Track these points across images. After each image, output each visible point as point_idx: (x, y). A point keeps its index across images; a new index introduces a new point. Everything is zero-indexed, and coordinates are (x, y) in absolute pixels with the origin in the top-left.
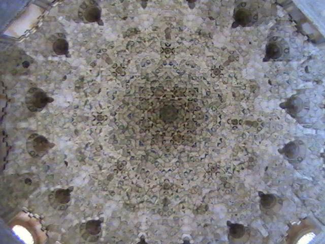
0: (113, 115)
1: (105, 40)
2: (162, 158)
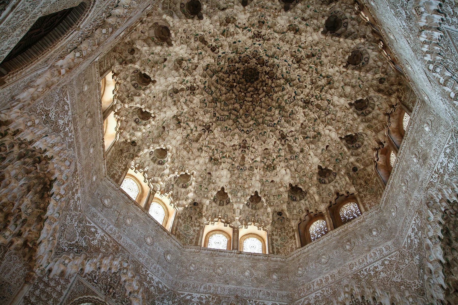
1: (231, 176)
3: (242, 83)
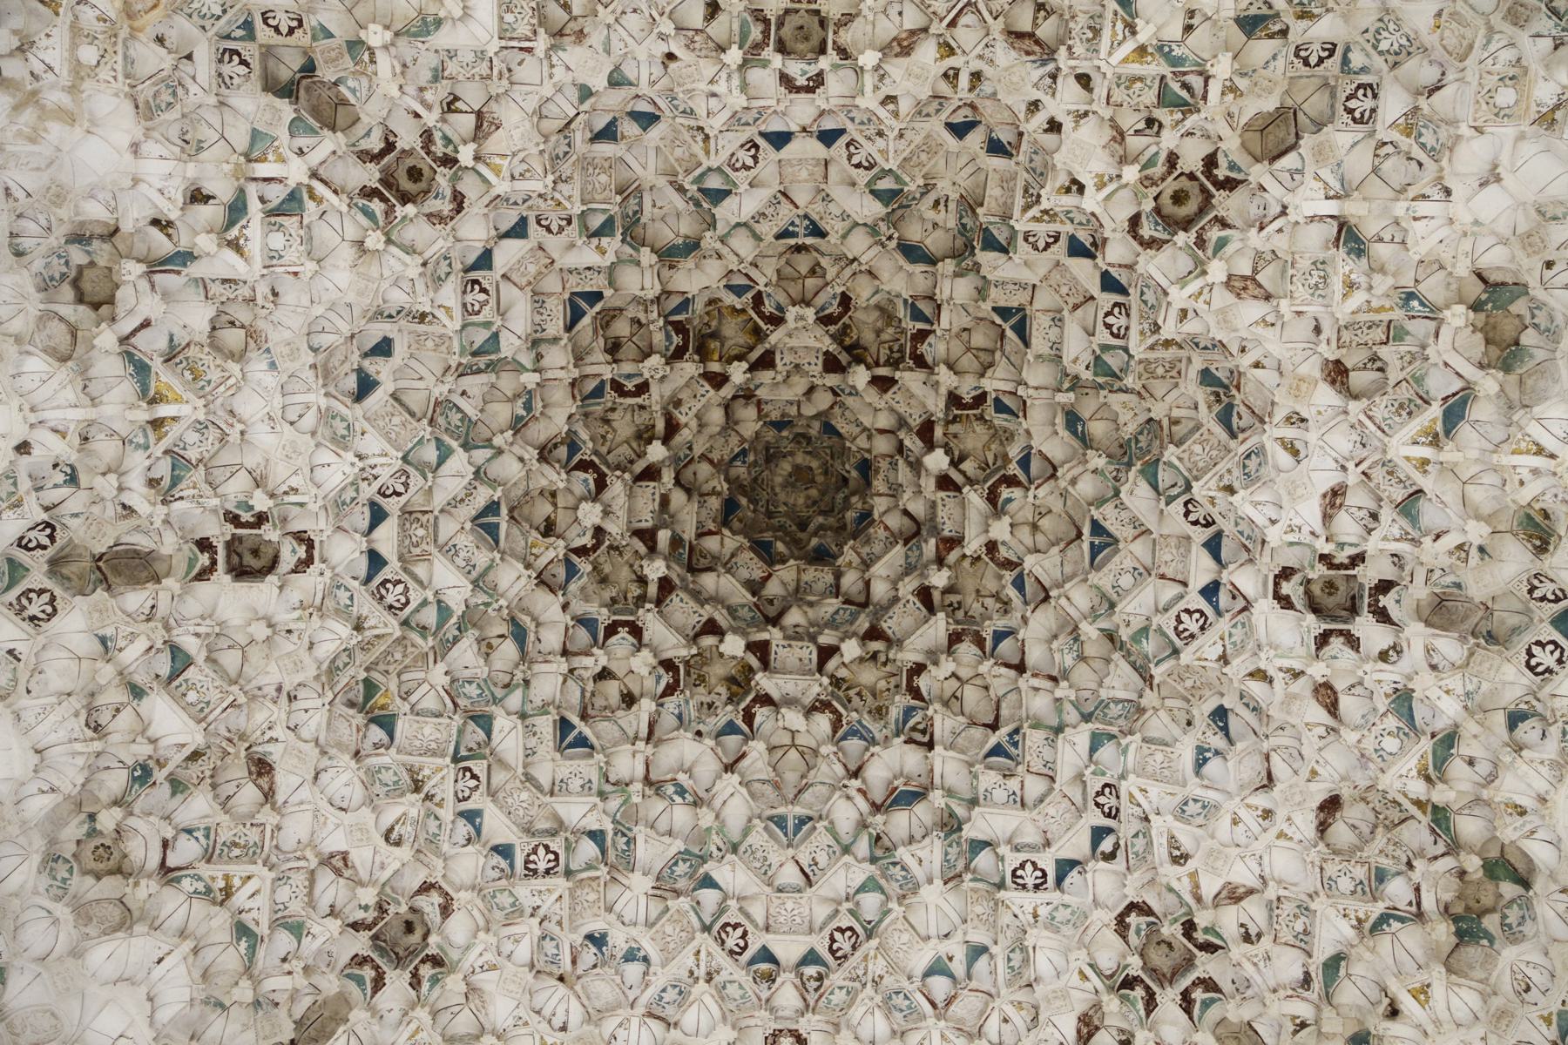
0: (1236, 593)
2: (844, 216)
3: (798, 594)
